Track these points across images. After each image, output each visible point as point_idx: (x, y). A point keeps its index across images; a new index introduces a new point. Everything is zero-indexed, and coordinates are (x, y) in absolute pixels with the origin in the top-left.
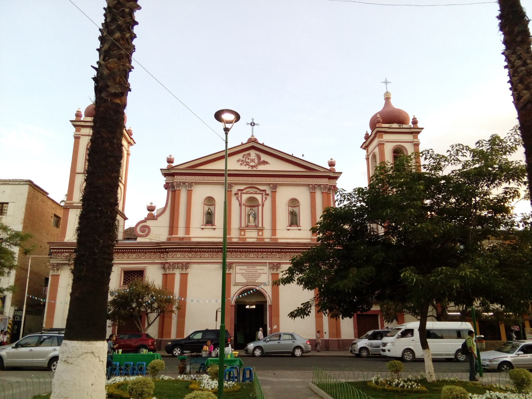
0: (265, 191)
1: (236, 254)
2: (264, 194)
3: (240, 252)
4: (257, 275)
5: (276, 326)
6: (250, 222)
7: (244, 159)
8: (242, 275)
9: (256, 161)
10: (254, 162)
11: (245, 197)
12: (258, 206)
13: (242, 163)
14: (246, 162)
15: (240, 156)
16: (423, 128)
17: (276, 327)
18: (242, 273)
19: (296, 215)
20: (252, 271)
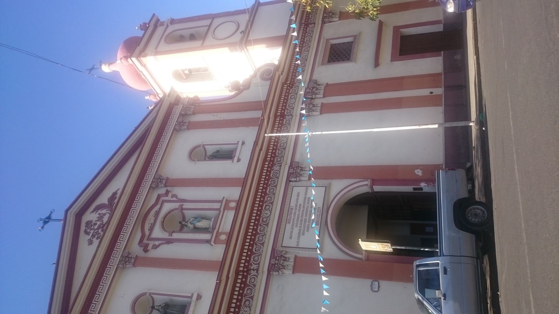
0: (159, 197)
1: (256, 245)
2: (166, 198)
3: (255, 235)
4: (306, 205)
5: (416, 171)
6: (208, 228)
7: (92, 232)
8: (303, 234)
9: (104, 211)
10: (105, 214)
11: (158, 233)
12: (182, 209)
13: (96, 237)
14: (98, 229)
15: (84, 239)
16: (154, 15)
17: (419, 170)
18: (299, 233)
19: (218, 151)
20: (299, 214)
